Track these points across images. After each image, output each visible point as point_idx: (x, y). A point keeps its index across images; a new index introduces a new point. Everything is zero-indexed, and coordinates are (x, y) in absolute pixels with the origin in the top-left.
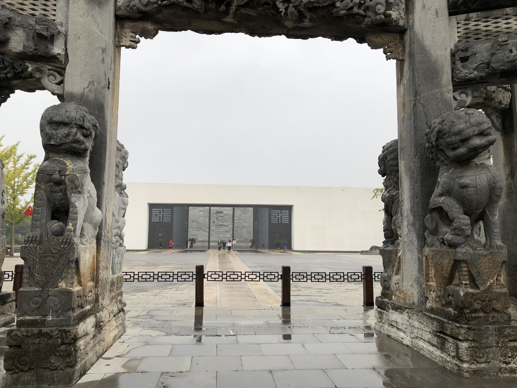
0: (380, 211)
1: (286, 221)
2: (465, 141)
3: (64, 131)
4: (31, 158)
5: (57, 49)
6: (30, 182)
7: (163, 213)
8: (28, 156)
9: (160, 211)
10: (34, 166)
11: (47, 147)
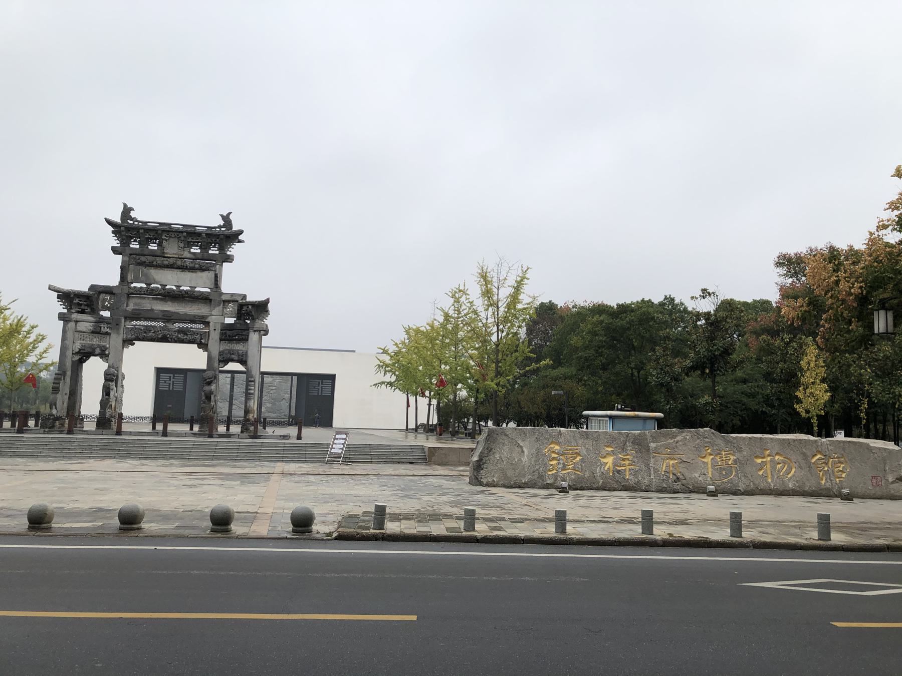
2: (206, 380)
4: (33, 327)
5: (107, 352)
7: (170, 382)
8: (30, 326)
9: (170, 377)
10: (36, 336)
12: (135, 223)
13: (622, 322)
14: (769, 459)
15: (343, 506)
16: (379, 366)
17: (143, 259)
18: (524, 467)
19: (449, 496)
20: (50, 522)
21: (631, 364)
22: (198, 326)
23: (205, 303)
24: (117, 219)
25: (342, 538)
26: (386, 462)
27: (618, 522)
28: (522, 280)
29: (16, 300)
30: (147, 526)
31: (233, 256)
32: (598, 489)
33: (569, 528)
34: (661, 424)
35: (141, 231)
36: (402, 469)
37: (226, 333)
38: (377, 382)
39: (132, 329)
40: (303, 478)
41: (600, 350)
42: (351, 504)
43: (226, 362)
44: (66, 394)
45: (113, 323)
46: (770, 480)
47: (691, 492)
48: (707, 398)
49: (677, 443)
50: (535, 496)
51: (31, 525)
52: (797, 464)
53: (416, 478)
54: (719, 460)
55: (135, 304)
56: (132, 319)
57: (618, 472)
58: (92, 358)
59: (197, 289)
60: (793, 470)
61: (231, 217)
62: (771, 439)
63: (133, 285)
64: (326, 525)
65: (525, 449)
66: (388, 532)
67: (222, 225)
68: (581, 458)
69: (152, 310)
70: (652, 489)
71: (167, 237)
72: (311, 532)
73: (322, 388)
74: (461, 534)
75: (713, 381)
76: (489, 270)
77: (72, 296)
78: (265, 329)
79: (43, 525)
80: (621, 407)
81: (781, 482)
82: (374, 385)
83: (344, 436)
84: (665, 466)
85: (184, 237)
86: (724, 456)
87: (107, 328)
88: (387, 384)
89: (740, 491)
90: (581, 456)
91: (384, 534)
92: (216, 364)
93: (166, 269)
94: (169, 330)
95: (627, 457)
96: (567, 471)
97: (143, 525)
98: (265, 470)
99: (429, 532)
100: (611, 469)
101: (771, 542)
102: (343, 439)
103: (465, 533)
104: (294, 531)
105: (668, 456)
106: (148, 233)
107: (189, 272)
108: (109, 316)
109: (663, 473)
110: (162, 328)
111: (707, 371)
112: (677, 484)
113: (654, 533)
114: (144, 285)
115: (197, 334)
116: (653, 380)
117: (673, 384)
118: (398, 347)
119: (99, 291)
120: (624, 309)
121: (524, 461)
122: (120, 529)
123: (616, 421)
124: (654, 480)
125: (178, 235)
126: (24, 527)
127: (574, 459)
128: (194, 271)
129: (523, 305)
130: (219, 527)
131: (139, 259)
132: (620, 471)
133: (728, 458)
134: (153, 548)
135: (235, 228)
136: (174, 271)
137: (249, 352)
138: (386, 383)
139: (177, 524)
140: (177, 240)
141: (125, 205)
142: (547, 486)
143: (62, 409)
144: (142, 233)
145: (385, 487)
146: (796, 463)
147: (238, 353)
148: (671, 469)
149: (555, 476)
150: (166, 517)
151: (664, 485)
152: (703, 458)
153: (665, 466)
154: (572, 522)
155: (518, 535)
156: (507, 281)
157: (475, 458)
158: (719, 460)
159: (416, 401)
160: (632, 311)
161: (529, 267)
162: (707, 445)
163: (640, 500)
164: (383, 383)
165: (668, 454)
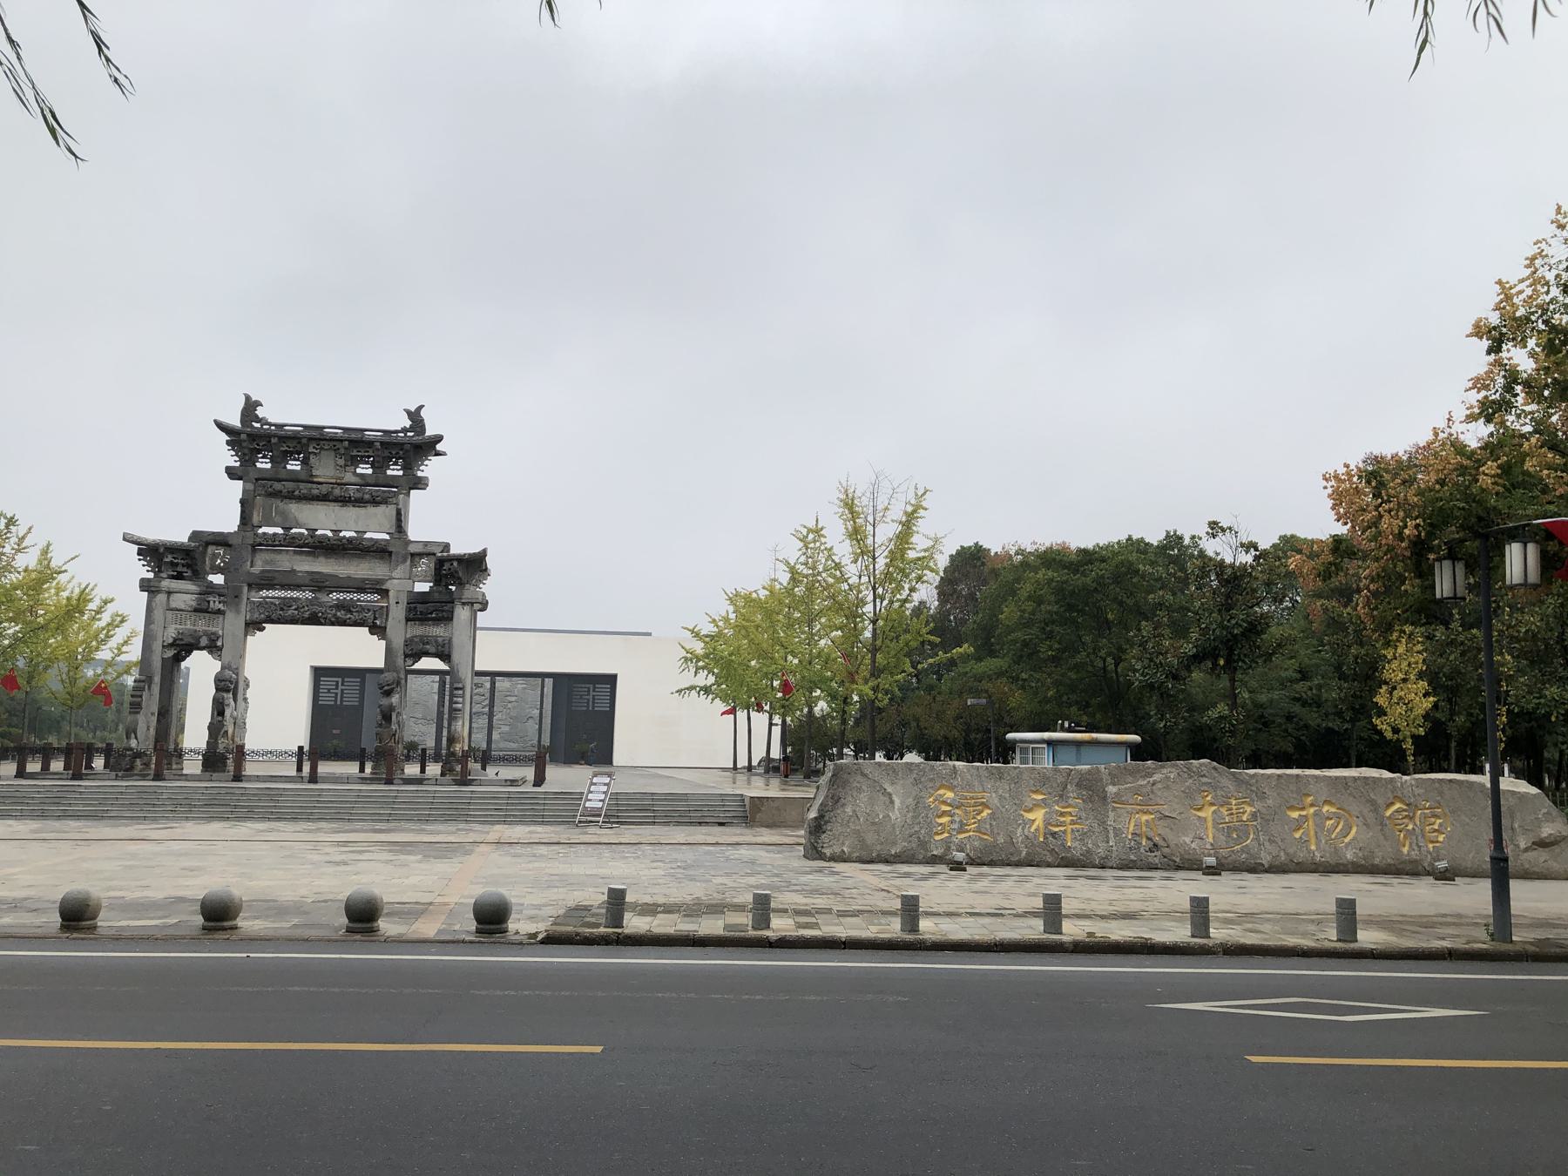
0: (672, 693)
1: (602, 706)
3: (223, 683)
4: (106, 602)
5: (219, 644)
6: (102, 641)
8: (101, 599)
9: (337, 682)
11: (216, 688)
12: (265, 427)
13: (1083, 578)
14: (1312, 810)
15: (575, 893)
16: (686, 659)
17: (278, 486)
18: (894, 828)
19: (761, 876)
20: (94, 918)
21: (1100, 651)
22: (369, 597)
23: (382, 558)
24: (235, 421)
25: (552, 940)
26: (679, 823)
27: (1017, 916)
28: (914, 511)
29: (77, 556)
30: (247, 924)
31: (427, 478)
32: (1018, 864)
33: (925, 925)
34: (1138, 753)
35: (274, 440)
36: (700, 834)
37: (415, 608)
38: (683, 687)
39: (260, 603)
40: (529, 849)
41: (1048, 629)
42: (590, 890)
43: (417, 656)
44: (153, 714)
45: (229, 595)
46: (1313, 847)
47: (1178, 868)
48: (1222, 708)
49: (1153, 785)
50: (907, 875)
51: (64, 923)
52: (1361, 818)
53: (718, 848)
54: (1226, 813)
55: (266, 562)
56: (261, 587)
57: (1054, 834)
58: (196, 653)
59: (368, 535)
60: (1354, 830)
61: (423, 413)
62: (1314, 775)
63: (261, 531)
64: (532, 922)
65: (895, 798)
66: (626, 931)
67: (408, 427)
68: (990, 811)
69: (293, 571)
70: (1110, 864)
71: (317, 449)
72: (507, 931)
73: (594, 699)
74: (743, 933)
75: (1233, 680)
76: (858, 494)
77: (162, 550)
78: (480, 600)
79: (84, 923)
80: (1070, 725)
81: (1333, 850)
82: (677, 692)
83: (607, 780)
84: (1132, 824)
85: (346, 448)
86: (1234, 807)
87: (220, 602)
88: (699, 691)
89: (1263, 865)
90: (989, 808)
91: (620, 934)
92: (400, 661)
93: (315, 503)
94: (321, 604)
95: (1068, 810)
96: (967, 835)
97: (239, 922)
98: (471, 837)
99: (695, 931)
100: (1042, 831)
101: (1252, 945)
102: (605, 784)
103: (752, 933)
104: (478, 931)
105: (1139, 807)
106: (284, 442)
107: (354, 506)
108: (222, 583)
109: (1130, 837)
110: (311, 602)
111: (1222, 662)
112: (1153, 854)
113: (1064, 931)
114: (279, 531)
115: (369, 610)
116: (1137, 679)
117: (1170, 686)
118: (718, 626)
119: (205, 541)
120: (1088, 558)
121: (893, 817)
122: (204, 929)
123: (1059, 748)
124: (1114, 848)
125: (335, 446)
126: (41, 919)
127: (977, 814)
128: (357, 504)
129: (917, 552)
130: (360, 925)
131: (271, 487)
132: (1055, 833)
133: (1241, 810)
134: (245, 955)
135: (430, 431)
136: (329, 506)
137: (455, 641)
138: (698, 689)
139: (295, 921)
140: (333, 453)
141: (248, 398)
142: (934, 860)
143: (147, 738)
144: (275, 444)
145: (659, 864)
146: (1358, 817)
147: (436, 641)
148: (1144, 829)
149: (947, 844)
150: (278, 910)
151: (1132, 857)
152: (1199, 810)
153: (1132, 824)
154: (940, 915)
155: (837, 934)
156: (888, 513)
157: (813, 814)
158: (1226, 813)
159: (749, 719)
160: (1103, 560)
161: (927, 488)
162: (1206, 788)
163: (1083, 881)
164: (692, 688)
165: (1140, 805)
